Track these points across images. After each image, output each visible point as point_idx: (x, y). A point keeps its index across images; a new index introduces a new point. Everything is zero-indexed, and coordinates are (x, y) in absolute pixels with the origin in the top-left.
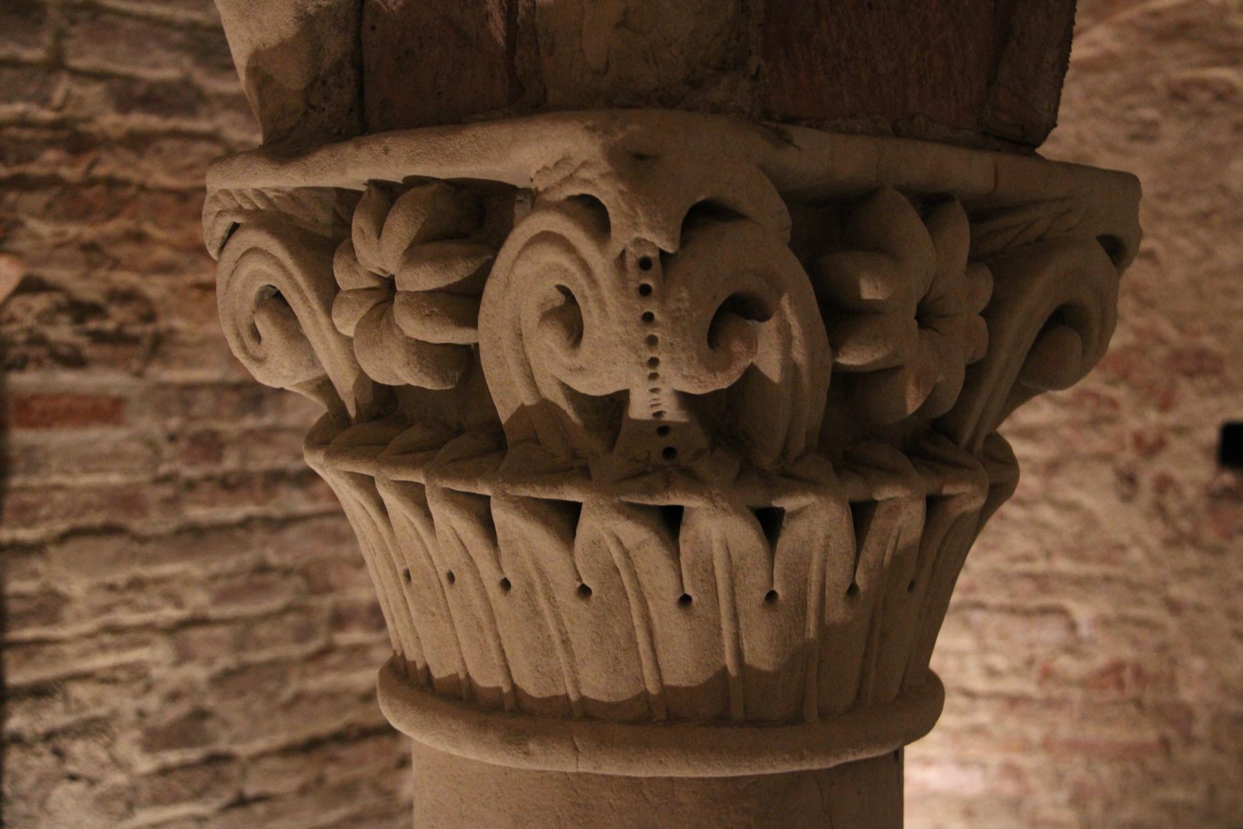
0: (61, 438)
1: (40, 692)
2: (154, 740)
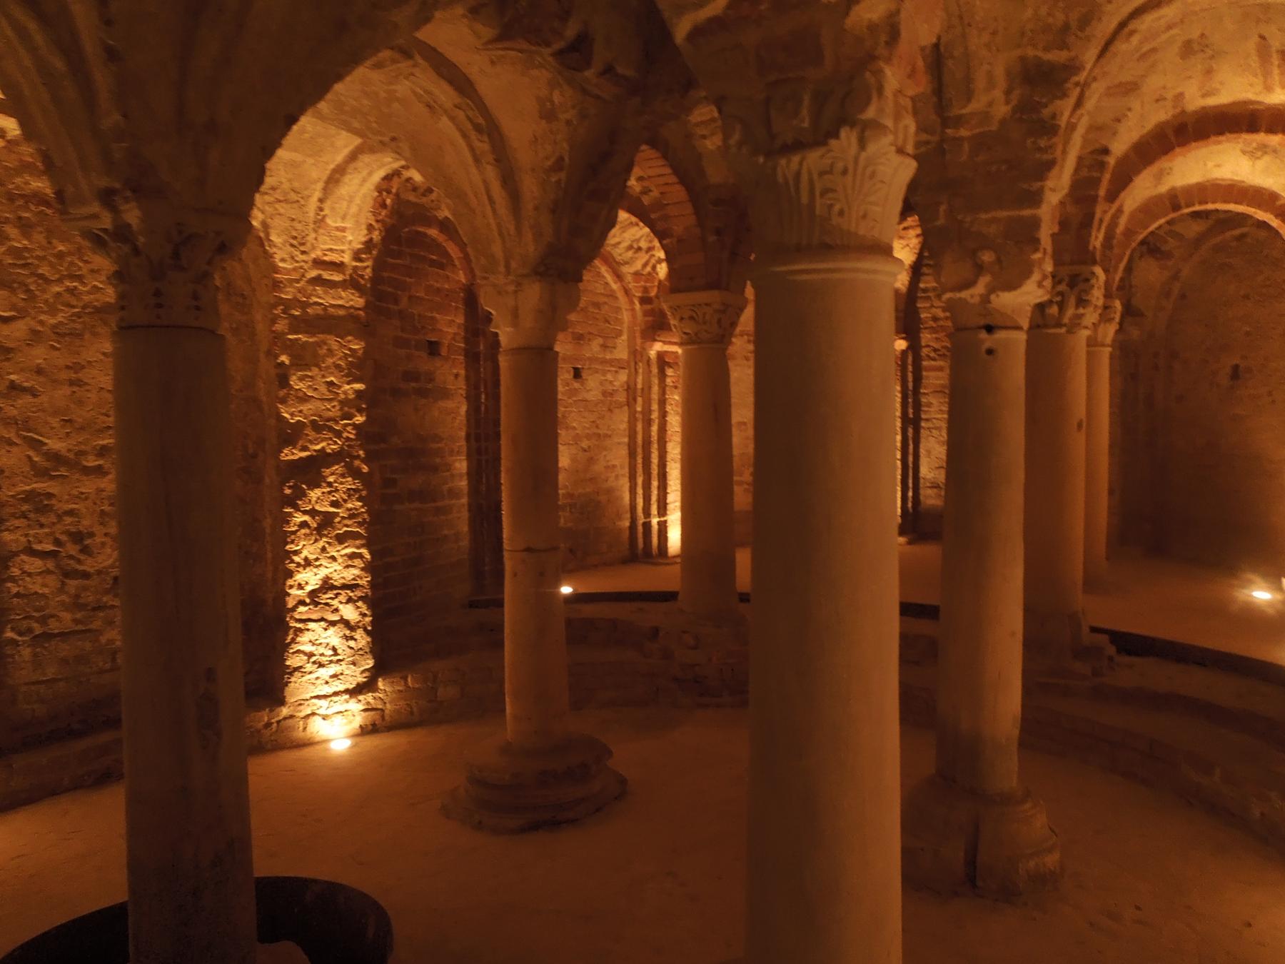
0: (932, 374)
1: (927, 420)
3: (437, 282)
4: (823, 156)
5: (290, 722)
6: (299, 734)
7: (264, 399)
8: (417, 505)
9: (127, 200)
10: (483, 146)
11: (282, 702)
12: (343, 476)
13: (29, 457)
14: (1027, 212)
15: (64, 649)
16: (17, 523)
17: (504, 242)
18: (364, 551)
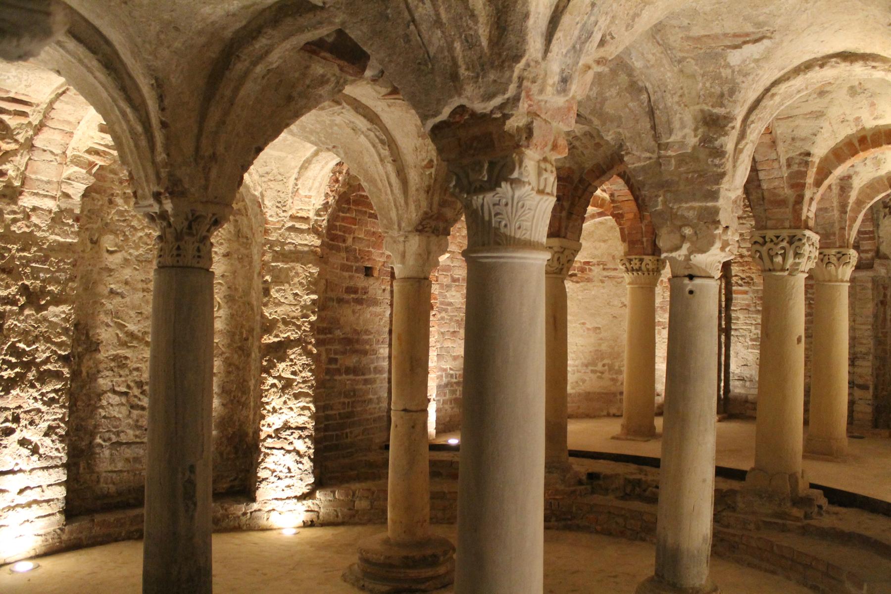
0: (739, 296)
2: (752, 340)
3: (373, 227)
4: (494, 196)
5: (258, 513)
6: (263, 522)
7: (255, 303)
8: (351, 377)
9: (166, 198)
10: (385, 152)
11: (254, 500)
12: (300, 355)
13: (117, 335)
14: (710, 204)
15: (128, 452)
16: (107, 373)
17: (397, 210)
18: (312, 406)
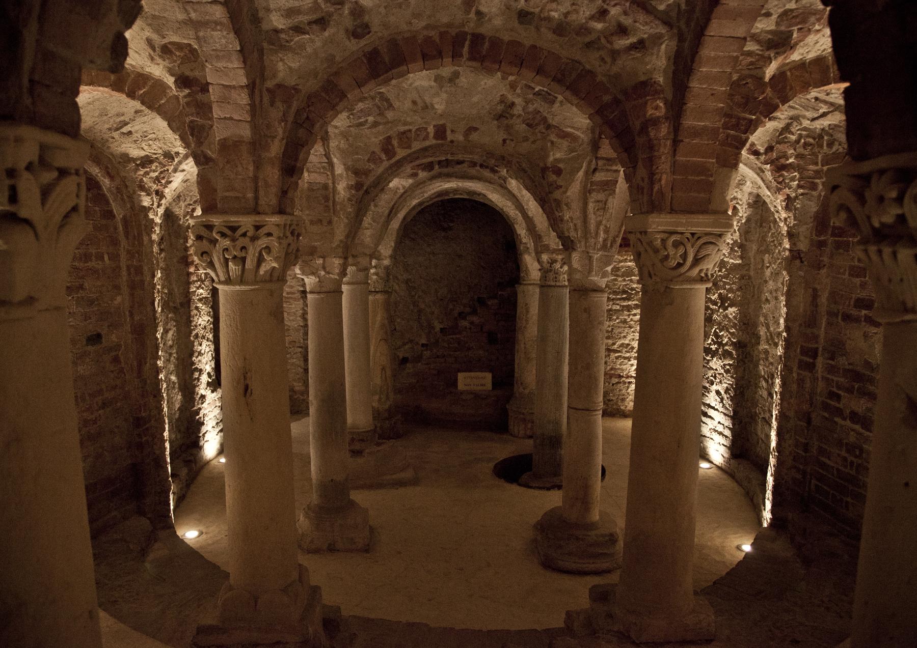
8: (857, 427)
